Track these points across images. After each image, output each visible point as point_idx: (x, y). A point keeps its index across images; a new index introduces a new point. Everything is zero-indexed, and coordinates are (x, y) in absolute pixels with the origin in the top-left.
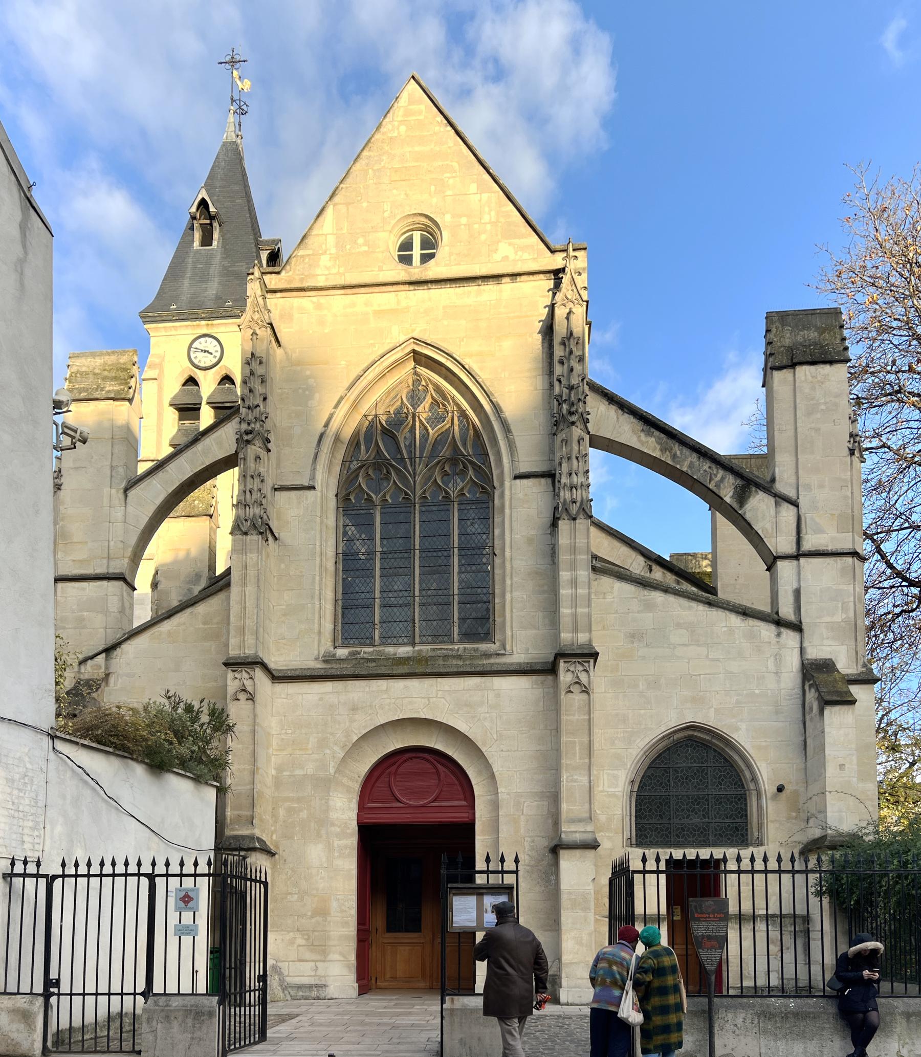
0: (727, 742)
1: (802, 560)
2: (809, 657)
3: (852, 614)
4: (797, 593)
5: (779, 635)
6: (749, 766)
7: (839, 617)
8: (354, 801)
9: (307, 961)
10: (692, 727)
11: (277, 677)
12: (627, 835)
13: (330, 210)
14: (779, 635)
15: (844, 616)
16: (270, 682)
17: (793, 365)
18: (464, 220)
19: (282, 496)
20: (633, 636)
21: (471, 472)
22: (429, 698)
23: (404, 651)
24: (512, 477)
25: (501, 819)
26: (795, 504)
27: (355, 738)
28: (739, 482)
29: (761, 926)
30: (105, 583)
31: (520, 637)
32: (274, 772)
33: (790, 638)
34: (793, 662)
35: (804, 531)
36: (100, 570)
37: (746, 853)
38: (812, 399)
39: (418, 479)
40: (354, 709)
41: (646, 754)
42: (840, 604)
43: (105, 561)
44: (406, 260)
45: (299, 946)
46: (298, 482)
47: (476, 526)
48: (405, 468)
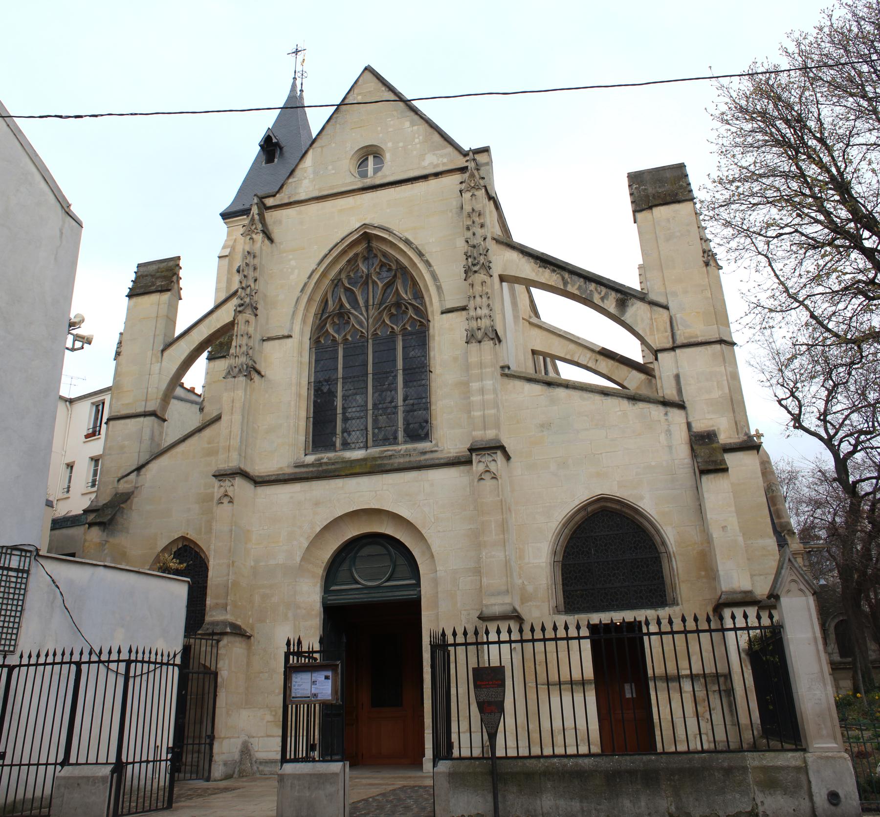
0: (636, 511)
1: (678, 351)
2: (695, 430)
3: (727, 391)
4: (677, 377)
5: (666, 414)
6: (657, 531)
7: (716, 394)
8: (319, 585)
9: (273, 736)
10: (602, 499)
11: (259, 482)
12: (553, 603)
13: (310, 153)
14: (666, 414)
15: (720, 393)
16: (252, 487)
17: (650, 208)
18: (401, 144)
19: (268, 345)
20: (542, 426)
22: (376, 492)
23: (357, 454)
24: (439, 312)
25: (440, 595)
26: (666, 308)
27: (318, 529)
28: (619, 295)
29: (687, 686)
30: (141, 419)
31: (449, 435)
32: (252, 564)
33: (677, 416)
34: (681, 437)
35: (676, 328)
36: (140, 409)
37: (664, 613)
38: (669, 229)
39: (371, 321)
40: (317, 504)
41: (566, 525)
42: (715, 383)
43: (144, 403)
44: (364, 175)
45: (268, 722)
46: (280, 333)
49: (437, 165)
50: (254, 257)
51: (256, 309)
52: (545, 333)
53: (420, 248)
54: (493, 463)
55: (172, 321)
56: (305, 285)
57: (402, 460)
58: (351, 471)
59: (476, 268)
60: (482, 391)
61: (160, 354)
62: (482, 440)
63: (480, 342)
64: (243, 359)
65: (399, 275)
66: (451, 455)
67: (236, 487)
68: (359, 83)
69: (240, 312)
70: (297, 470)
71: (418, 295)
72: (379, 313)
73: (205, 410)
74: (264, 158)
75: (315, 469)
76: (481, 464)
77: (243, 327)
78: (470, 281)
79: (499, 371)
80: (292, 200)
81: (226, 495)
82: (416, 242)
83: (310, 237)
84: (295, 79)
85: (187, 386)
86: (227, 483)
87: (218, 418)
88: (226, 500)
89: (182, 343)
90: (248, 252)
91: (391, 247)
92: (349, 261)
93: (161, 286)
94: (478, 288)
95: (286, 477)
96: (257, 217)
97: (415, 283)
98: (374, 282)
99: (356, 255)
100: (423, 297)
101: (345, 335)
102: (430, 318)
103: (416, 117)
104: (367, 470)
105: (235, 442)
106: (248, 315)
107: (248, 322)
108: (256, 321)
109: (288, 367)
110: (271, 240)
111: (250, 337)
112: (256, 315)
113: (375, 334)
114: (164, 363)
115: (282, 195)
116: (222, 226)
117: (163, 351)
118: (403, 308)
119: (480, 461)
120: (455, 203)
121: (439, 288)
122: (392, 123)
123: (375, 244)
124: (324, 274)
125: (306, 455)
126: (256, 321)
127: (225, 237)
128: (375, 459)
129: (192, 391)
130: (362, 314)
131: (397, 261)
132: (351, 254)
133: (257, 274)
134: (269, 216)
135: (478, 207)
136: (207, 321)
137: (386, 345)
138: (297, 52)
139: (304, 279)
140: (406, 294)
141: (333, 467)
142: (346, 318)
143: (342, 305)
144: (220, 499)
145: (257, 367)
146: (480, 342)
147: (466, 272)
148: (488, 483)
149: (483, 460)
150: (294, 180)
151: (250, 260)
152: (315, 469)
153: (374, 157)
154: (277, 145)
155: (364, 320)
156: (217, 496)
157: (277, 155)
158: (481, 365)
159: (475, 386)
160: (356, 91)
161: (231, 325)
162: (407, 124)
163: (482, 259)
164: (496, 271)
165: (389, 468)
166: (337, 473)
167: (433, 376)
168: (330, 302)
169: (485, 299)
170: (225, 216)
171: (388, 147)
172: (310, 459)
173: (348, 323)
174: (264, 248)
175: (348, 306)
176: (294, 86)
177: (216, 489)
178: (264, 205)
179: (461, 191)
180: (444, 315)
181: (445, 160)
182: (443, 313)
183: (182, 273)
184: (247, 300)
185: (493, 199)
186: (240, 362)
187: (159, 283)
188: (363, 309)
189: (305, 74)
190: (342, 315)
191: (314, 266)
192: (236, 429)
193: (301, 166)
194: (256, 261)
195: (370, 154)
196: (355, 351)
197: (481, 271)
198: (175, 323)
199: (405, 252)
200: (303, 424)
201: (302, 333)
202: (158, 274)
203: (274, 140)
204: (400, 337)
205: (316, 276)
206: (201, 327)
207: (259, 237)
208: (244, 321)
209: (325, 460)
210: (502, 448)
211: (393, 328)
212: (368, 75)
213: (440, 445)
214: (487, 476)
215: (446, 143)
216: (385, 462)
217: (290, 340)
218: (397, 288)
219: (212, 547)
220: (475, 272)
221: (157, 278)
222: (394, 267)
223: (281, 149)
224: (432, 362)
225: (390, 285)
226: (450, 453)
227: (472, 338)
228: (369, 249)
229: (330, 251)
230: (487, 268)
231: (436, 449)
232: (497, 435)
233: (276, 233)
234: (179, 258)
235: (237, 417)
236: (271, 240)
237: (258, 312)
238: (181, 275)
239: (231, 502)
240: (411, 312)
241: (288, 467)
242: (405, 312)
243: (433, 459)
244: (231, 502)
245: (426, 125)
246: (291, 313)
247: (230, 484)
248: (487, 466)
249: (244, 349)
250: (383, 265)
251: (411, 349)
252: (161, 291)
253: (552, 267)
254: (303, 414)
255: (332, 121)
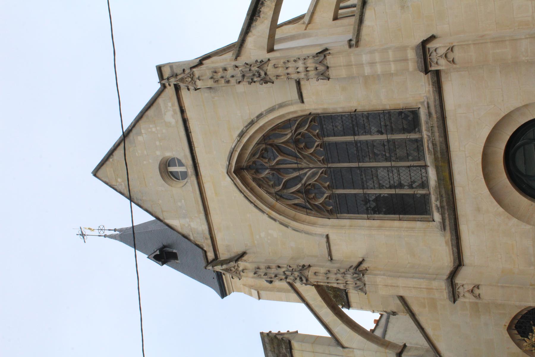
11: (459, 262)
18: (158, 143)
20: (403, 7)
21: (303, 130)
23: (432, 174)
24: (302, 105)
27: (501, 209)
39: (311, 166)
40: (478, 210)
44: (184, 175)
46: (325, 245)
47: (337, 124)
48: (306, 174)
49: (174, 111)
50: (258, 268)
51: (304, 266)
52: (318, 9)
53: (246, 124)
54: (438, 51)
55: (316, 340)
56: (281, 223)
57: (437, 134)
58: (448, 179)
59: (263, 74)
60: (372, 64)
61: (346, 350)
62: (417, 62)
63: (328, 68)
64: (349, 277)
65: (270, 142)
66: (431, 89)
67: (464, 283)
68: (107, 180)
69: (307, 280)
70: (448, 228)
71: (286, 124)
72: (305, 158)
73: (395, 310)
74: (173, 261)
75: (446, 212)
76: (439, 62)
77: (320, 278)
78: (274, 79)
79: (353, 49)
80: (208, 237)
81: (472, 291)
82: (241, 127)
83: (240, 220)
84: (105, 236)
85: (372, 326)
86: (461, 290)
87: (402, 299)
88: (477, 292)
89: (335, 330)
90: (255, 273)
91: (246, 149)
92: (260, 186)
93: (286, 349)
94: (280, 71)
95: (454, 238)
96: (224, 267)
97: (277, 127)
98: (278, 163)
99: (254, 180)
100: (290, 120)
101: (325, 187)
102: (307, 113)
103: (134, 131)
104: (446, 165)
105: (424, 283)
106: (310, 274)
107: (315, 273)
108: (314, 266)
109: (354, 238)
110: (243, 254)
111: (329, 271)
112: (309, 266)
113: (323, 161)
114: (354, 346)
115: (204, 245)
116: (233, 297)
117: (343, 347)
118: (299, 137)
119: (437, 63)
120: (206, 95)
121: (281, 106)
122: (139, 152)
123: (244, 164)
124: (272, 208)
125: (434, 221)
126: (314, 266)
127: (242, 294)
128: (436, 159)
129: (377, 322)
130: (306, 174)
131: (258, 144)
132: (254, 184)
133: (273, 266)
134: (223, 255)
135: (209, 74)
136: (316, 309)
137: (331, 152)
138: (83, 235)
139: (277, 224)
140: (287, 134)
141: (444, 195)
142: (309, 187)
143: (298, 191)
144: (475, 297)
145: (355, 264)
146: (328, 68)
147: (266, 82)
148: (457, 55)
149: (435, 60)
150: (191, 235)
151: (261, 272)
152: (446, 212)
153: (169, 166)
154: (162, 250)
155: (311, 171)
156: (473, 300)
157: (170, 250)
158: (349, 65)
159: (367, 70)
160: (114, 183)
161: (318, 287)
162: (140, 138)
163: (254, 69)
164: (264, 55)
165: (444, 146)
166: (450, 193)
167: (359, 109)
168: (296, 201)
169: (289, 65)
170: (223, 294)
171: (160, 154)
172: (437, 216)
173: (314, 185)
174: (250, 260)
175: (299, 186)
176: (111, 237)
177: (467, 300)
178: (213, 260)
179: (196, 90)
180: (305, 100)
181: (170, 104)
182: (303, 102)
183: (275, 331)
184: (296, 274)
185: (201, 61)
186: (352, 280)
187: (284, 351)
188: (302, 172)
189: (101, 227)
190: (306, 191)
191: (265, 217)
192: (412, 283)
193: (180, 230)
194: (262, 266)
195: (167, 169)
196: (337, 178)
197: (265, 68)
198: (318, 336)
199: (250, 137)
200: (405, 224)
201: (323, 226)
202: (276, 351)
203: (158, 252)
204: (326, 139)
205: (274, 214)
206: (321, 314)
207: (242, 264)
208: (315, 277)
209: (438, 203)
210: (424, 43)
211: (317, 146)
212: (99, 174)
213: (422, 100)
214: (451, 56)
215: (155, 104)
216: (439, 149)
217: (331, 237)
218: (282, 143)
219: (517, 303)
220: (266, 74)
221: (280, 352)
222: (264, 146)
223: (164, 247)
224: (347, 110)
225: (280, 149)
226: (429, 91)
227: (324, 75)
228: (248, 168)
229: (251, 202)
230: (262, 64)
231: (426, 104)
232: (412, 49)
233: (237, 250)
234: (262, 334)
235: (401, 282)
236: (243, 254)
237: (307, 264)
238: (277, 332)
239: (478, 287)
240: (303, 130)
241: (445, 236)
242: (303, 135)
243: (435, 106)
244: (478, 287)
245: (140, 122)
246: (306, 235)
247: (461, 288)
248: (441, 56)
249: (339, 276)
250: (262, 156)
251: (336, 129)
252: (291, 349)
253: (259, 6)
254: (397, 223)
255: (140, 203)
